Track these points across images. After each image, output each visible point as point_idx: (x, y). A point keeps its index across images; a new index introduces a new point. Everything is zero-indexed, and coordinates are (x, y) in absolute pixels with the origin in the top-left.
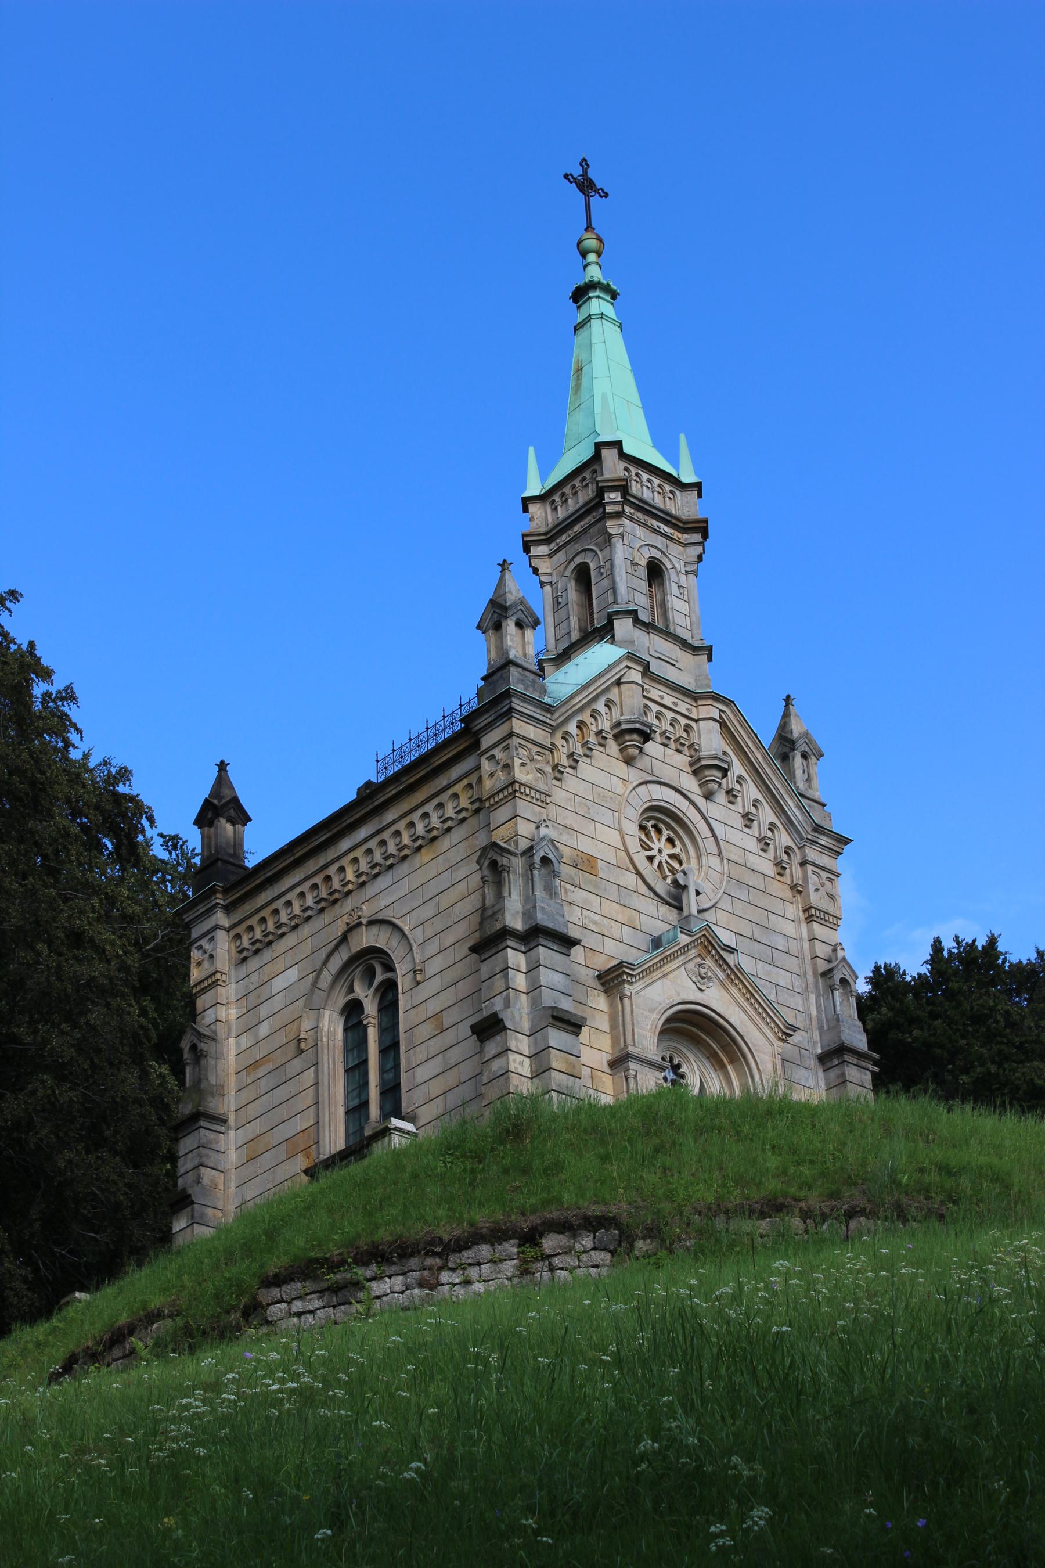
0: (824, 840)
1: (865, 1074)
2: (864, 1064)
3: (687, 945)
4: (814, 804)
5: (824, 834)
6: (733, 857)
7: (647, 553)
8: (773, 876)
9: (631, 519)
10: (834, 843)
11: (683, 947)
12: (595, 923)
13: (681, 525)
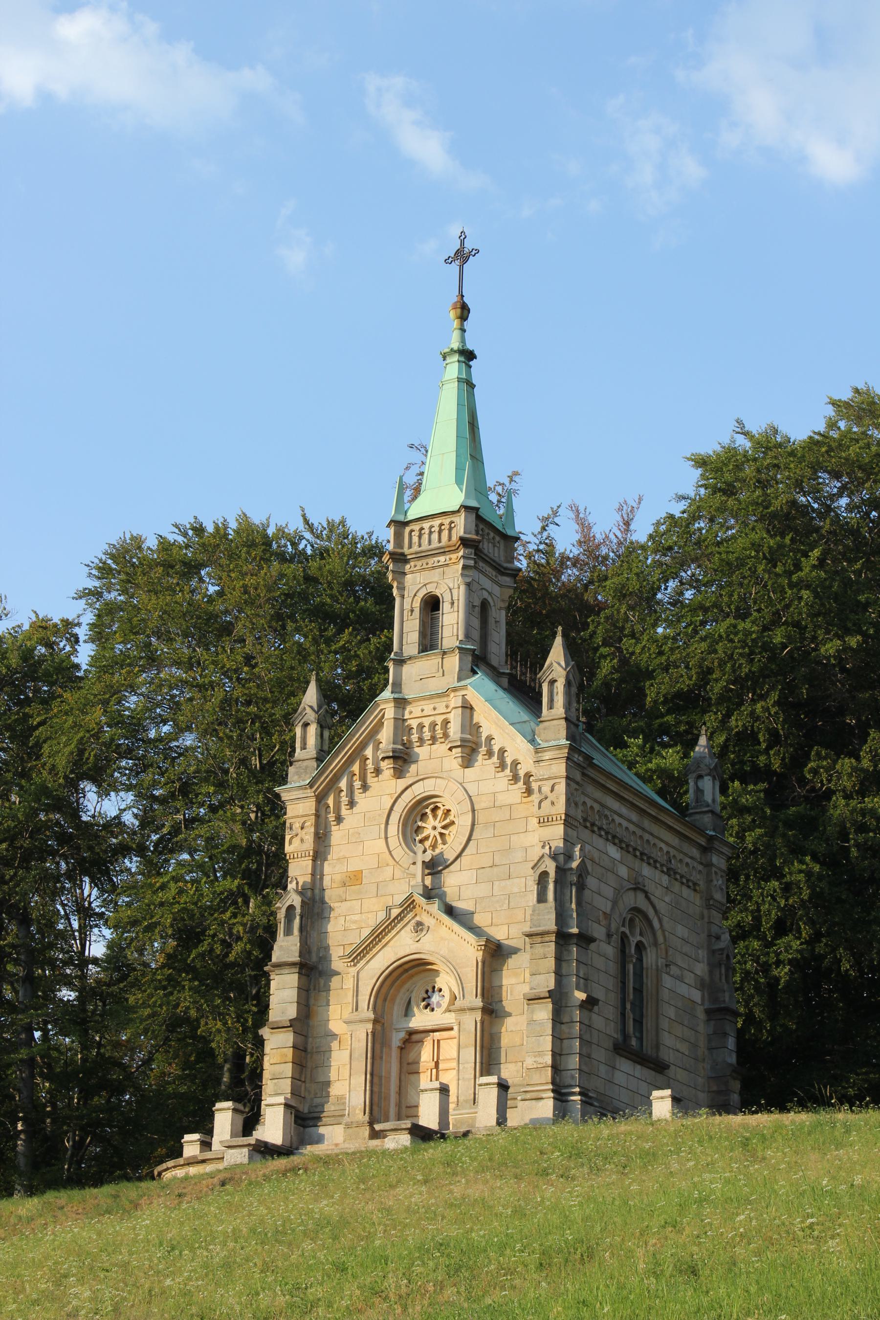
0: (547, 755)
1: (549, 946)
2: (547, 939)
3: (399, 914)
4: (555, 722)
5: (545, 751)
6: (483, 805)
7: (421, 595)
8: (519, 801)
9: (412, 572)
10: (558, 752)
11: (396, 918)
12: (355, 922)
13: (453, 548)
